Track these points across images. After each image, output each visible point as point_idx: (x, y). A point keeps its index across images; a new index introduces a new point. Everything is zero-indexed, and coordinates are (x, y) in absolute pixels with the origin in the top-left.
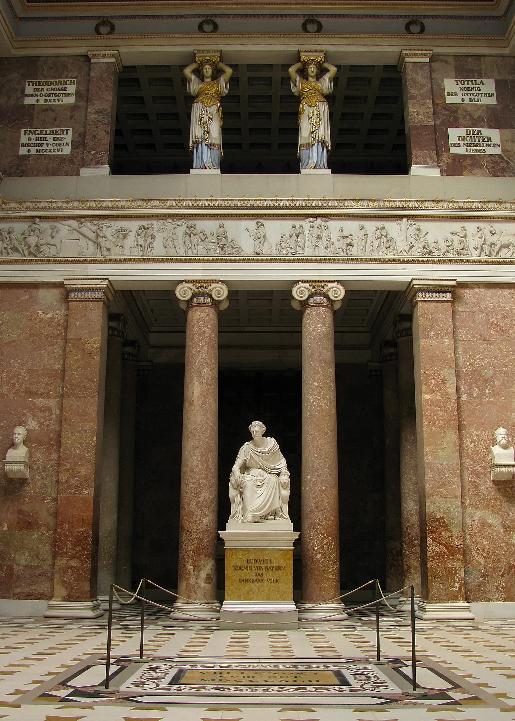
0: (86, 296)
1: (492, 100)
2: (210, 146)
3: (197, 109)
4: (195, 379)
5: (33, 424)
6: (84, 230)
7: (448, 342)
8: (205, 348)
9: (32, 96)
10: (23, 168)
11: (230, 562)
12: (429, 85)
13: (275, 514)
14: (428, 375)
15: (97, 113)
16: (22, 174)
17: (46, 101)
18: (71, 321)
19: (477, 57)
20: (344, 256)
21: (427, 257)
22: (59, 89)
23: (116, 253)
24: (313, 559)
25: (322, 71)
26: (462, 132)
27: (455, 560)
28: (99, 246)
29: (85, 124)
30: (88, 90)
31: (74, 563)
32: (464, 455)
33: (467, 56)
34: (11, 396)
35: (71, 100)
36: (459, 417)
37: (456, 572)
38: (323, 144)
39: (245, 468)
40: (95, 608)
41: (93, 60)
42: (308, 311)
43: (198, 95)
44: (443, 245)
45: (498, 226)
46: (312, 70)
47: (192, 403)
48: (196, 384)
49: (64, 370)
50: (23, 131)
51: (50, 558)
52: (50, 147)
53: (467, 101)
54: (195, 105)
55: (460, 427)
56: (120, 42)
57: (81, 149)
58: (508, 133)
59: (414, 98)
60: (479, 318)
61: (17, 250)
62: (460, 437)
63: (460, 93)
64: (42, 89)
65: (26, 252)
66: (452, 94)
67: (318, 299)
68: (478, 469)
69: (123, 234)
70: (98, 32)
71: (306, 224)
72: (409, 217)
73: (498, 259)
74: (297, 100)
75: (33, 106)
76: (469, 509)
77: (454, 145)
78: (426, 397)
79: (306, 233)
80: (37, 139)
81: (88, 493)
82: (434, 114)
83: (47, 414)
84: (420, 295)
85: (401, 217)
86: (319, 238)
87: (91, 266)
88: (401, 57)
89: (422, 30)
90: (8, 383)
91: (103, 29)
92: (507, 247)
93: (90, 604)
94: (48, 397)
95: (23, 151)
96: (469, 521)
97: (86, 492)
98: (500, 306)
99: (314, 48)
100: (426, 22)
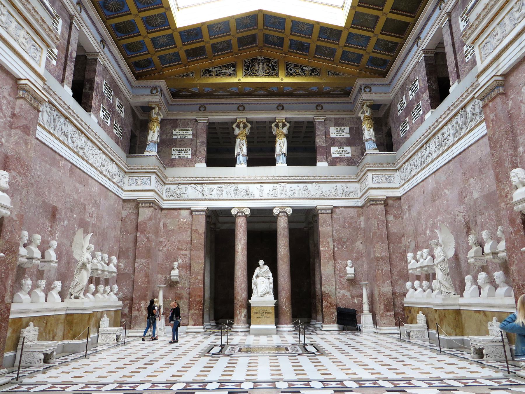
0: (199, 213)
1: (348, 135)
3: (238, 141)
4: (239, 243)
6: (197, 188)
7: (330, 229)
8: (242, 232)
9: (176, 135)
10: (173, 163)
11: (253, 311)
12: (324, 130)
13: (268, 293)
14: (322, 241)
15: (200, 142)
16: (173, 166)
17: (181, 137)
18: (194, 222)
19: (343, 118)
20: (292, 197)
21: (323, 197)
22: (186, 133)
23: (209, 197)
24: (282, 308)
25: (284, 125)
26: (336, 148)
27: (333, 309)
28: (203, 194)
29: (196, 146)
30: (197, 133)
31: (197, 312)
32: (336, 270)
33: (339, 118)
34: (172, 250)
35: (190, 137)
37: (334, 313)
38: (284, 154)
39: (257, 277)
40: (204, 328)
41: (198, 121)
42: (279, 218)
43: (238, 136)
45: (349, 185)
46: (280, 125)
47: (238, 252)
48: (239, 245)
49: (191, 240)
50: (173, 149)
52: (183, 155)
53: (338, 136)
54: (237, 139)
55: (335, 260)
56: (208, 114)
57: (195, 156)
58: (354, 148)
59: (318, 135)
60: (341, 219)
61: (173, 196)
62: (334, 263)
63: (336, 133)
64: (179, 133)
65: (176, 197)
67: (283, 214)
68: (341, 275)
70: (200, 110)
72: (316, 182)
73: (349, 197)
74: (275, 137)
76: (338, 290)
77: (333, 153)
78: (321, 249)
79: (278, 189)
80: (178, 152)
81: (201, 286)
83: (185, 257)
84: (320, 212)
85: (313, 182)
88: (314, 119)
89: (322, 108)
90: (170, 245)
91: (202, 109)
92: (352, 192)
93: (203, 327)
94: (186, 250)
95: (173, 157)
96: (338, 294)
97: (200, 285)
98: (349, 215)
99: (281, 116)
100: (323, 105)
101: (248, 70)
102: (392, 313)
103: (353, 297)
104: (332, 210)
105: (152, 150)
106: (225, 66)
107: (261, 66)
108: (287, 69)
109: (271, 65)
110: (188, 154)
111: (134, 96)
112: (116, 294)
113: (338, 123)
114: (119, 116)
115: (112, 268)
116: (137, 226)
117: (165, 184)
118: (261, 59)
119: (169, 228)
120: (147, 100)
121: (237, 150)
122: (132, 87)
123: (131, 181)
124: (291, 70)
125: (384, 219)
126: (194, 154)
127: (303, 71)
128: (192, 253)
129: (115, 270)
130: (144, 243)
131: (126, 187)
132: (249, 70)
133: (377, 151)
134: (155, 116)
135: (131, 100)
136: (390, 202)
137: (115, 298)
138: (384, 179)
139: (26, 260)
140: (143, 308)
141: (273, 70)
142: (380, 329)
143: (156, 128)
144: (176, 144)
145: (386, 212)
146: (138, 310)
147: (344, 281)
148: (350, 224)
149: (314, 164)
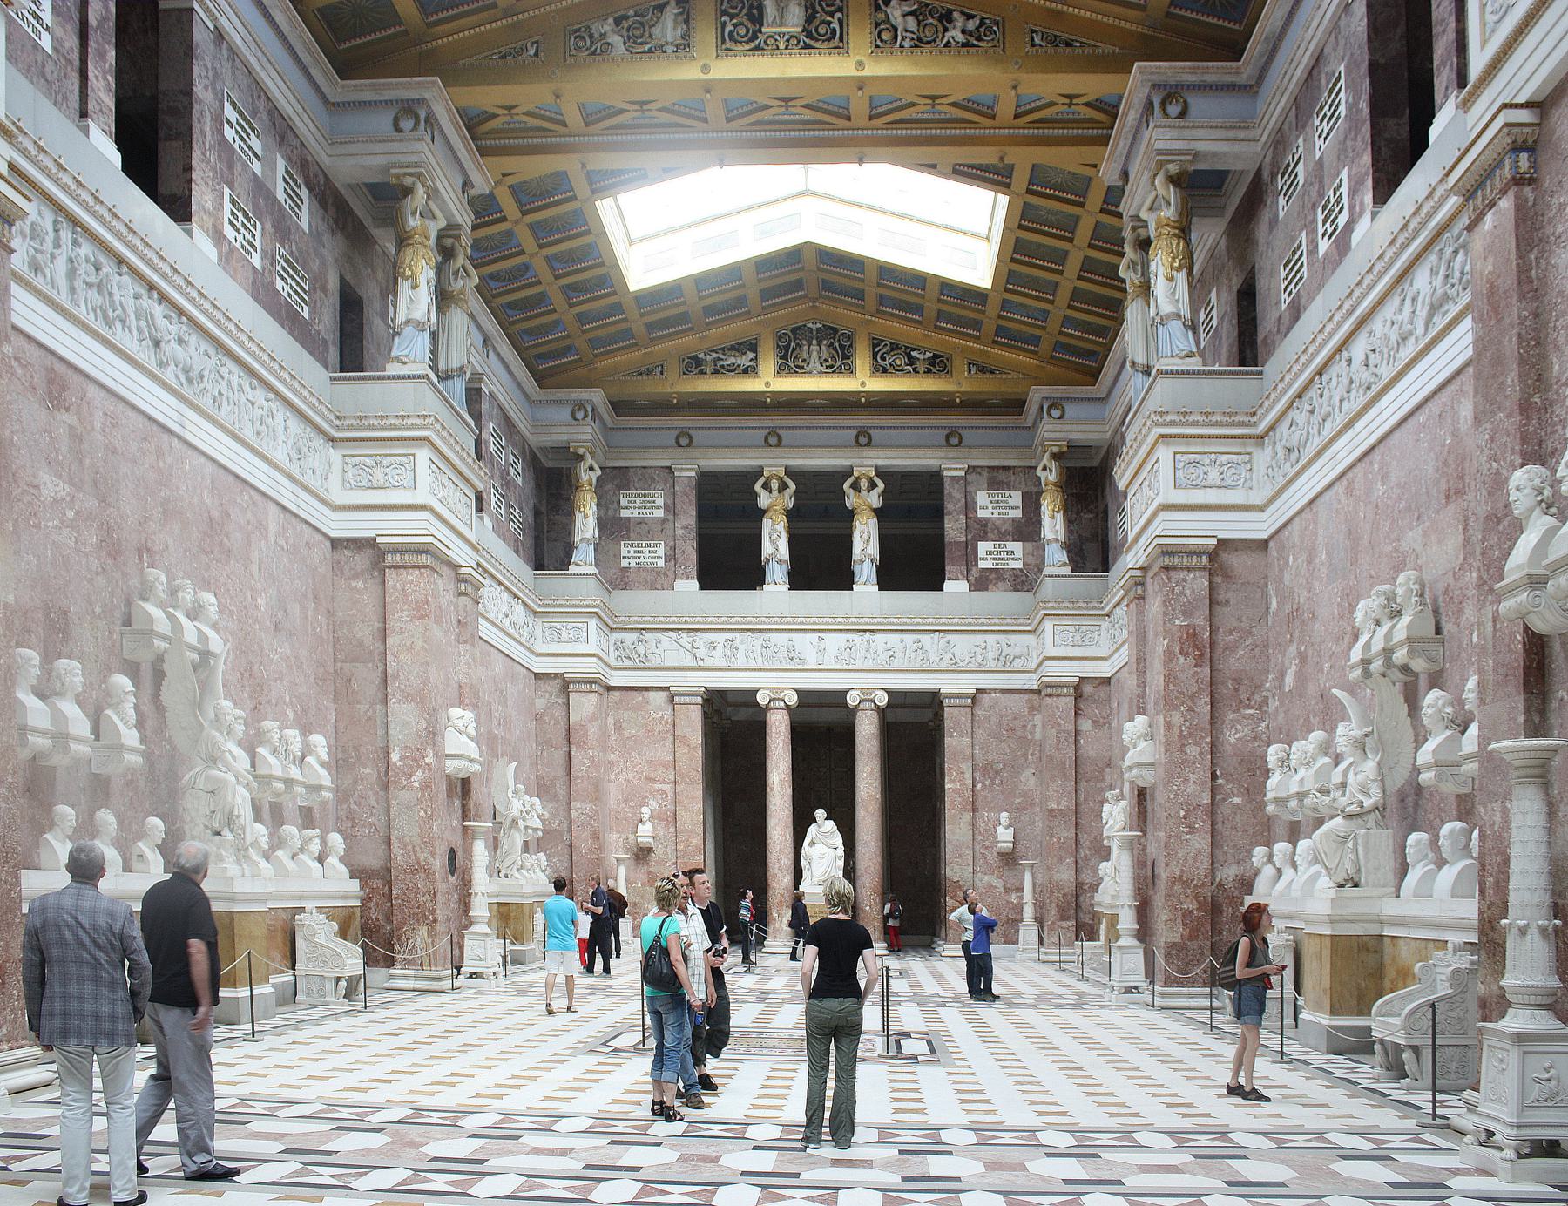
3: (766, 524)
35: (660, 513)
56: (697, 455)
74: (850, 515)
110: (653, 555)
120: (565, 437)
121: (767, 549)
139: (283, 786)
142: (1046, 954)
147: (992, 857)
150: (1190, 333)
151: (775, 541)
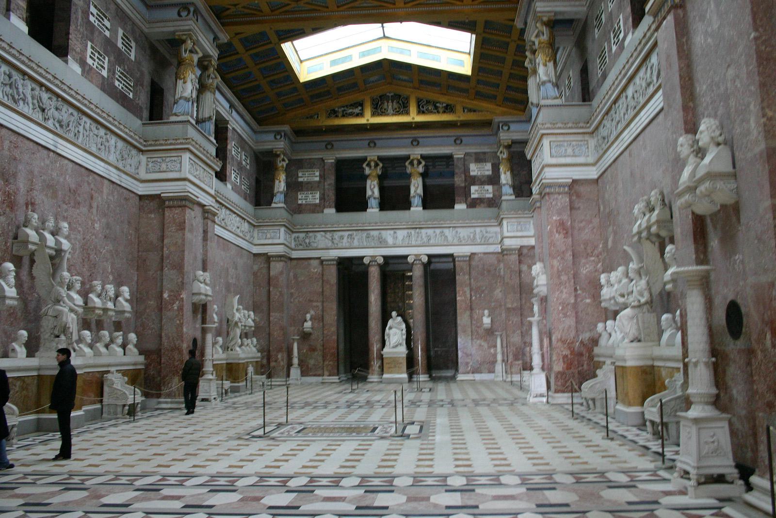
0: (329, 263)
1: (490, 173)
2: (375, 198)
3: (369, 182)
5: (312, 312)
6: (327, 236)
7: (467, 277)
13: (401, 344)
16: (300, 212)
19: (484, 153)
23: (340, 245)
25: (419, 163)
28: (333, 242)
29: (324, 190)
31: (331, 363)
35: (317, 179)
36: (471, 306)
38: (420, 196)
39: (390, 328)
40: (339, 379)
44: (466, 237)
45: (489, 229)
46: (415, 162)
49: (323, 292)
51: (322, 361)
55: (471, 309)
58: (496, 187)
61: (301, 245)
62: (471, 313)
66: (472, 171)
68: (479, 325)
69: (342, 237)
70: (327, 148)
71: (413, 231)
75: (302, 182)
78: (458, 298)
81: (335, 337)
82: (465, 180)
85: (450, 227)
86: (418, 237)
87: (331, 251)
93: (337, 377)
95: (300, 202)
99: (416, 153)
101: (376, 108)
102: (520, 362)
103: (489, 347)
104: (470, 256)
105: (279, 201)
106: (351, 105)
107: (390, 104)
108: (418, 106)
109: (401, 102)
110: (314, 198)
111: (257, 142)
112: (255, 347)
113: (480, 158)
114: (246, 169)
115: (250, 322)
116: (269, 280)
117: (293, 232)
118: (390, 95)
119: (299, 279)
121: (369, 193)
122: (255, 132)
123: (260, 234)
124: (423, 107)
125: (517, 269)
126: (322, 198)
127: (436, 108)
128: (325, 305)
129: (252, 324)
130: (277, 297)
131: (256, 241)
132: (378, 110)
133: (513, 197)
134: (280, 165)
135: (254, 148)
136: (525, 251)
137: (254, 349)
138: (519, 228)
140: (280, 359)
141: (403, 109)
143: (282, 177)
144: (302, 186)
145: (520, 262)
146: (276, 361)
148: (489, 271)
149: (453, 207)
150: (556, 89)
151: (373, 189)
